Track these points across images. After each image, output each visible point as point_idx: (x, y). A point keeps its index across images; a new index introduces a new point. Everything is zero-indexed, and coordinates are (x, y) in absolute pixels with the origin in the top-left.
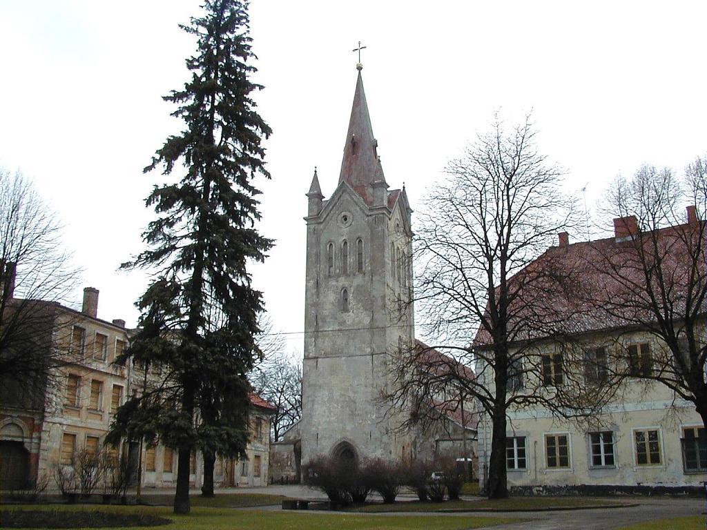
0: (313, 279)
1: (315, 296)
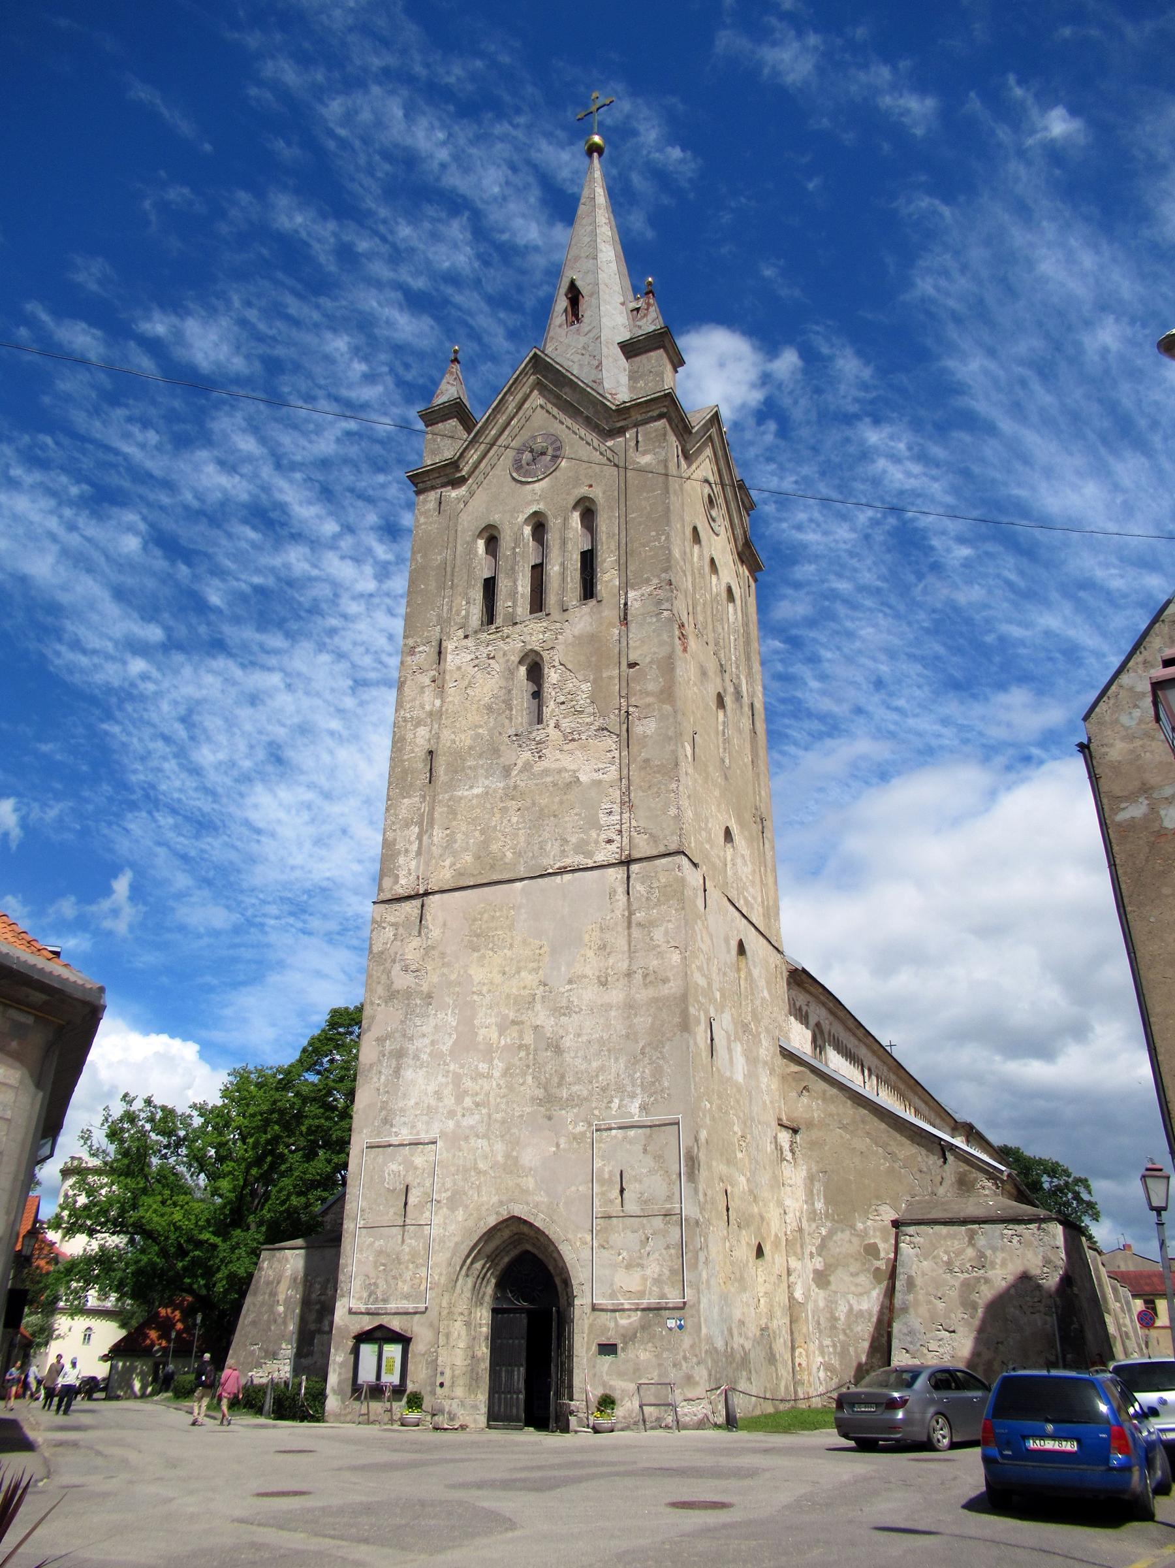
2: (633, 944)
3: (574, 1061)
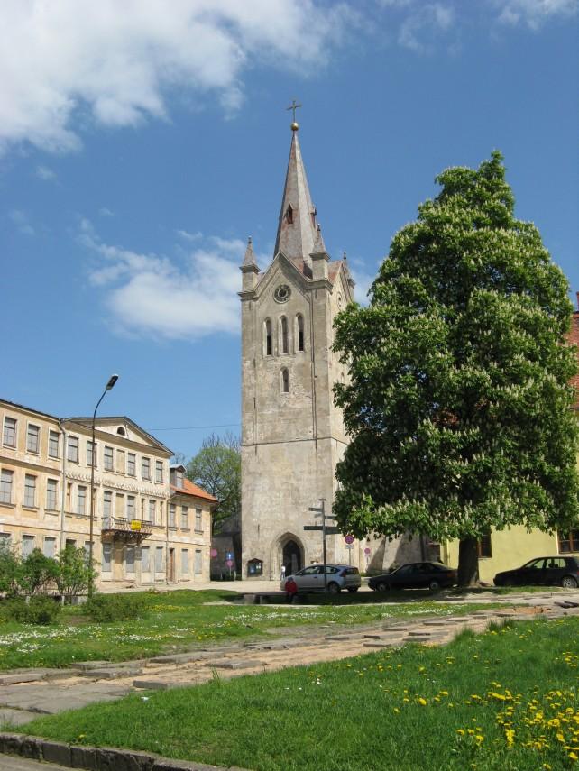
0: (250, 359)
1: (252, 378)
3: (303, 494)
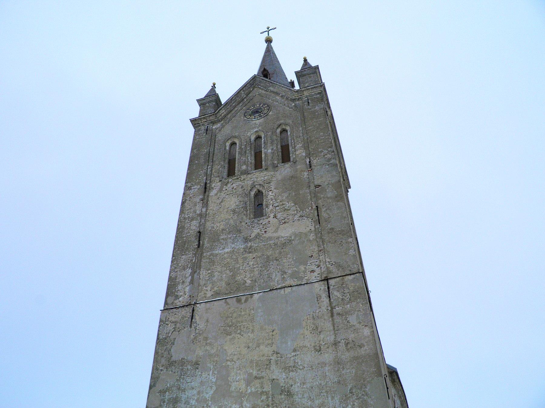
2: (335, 326)
